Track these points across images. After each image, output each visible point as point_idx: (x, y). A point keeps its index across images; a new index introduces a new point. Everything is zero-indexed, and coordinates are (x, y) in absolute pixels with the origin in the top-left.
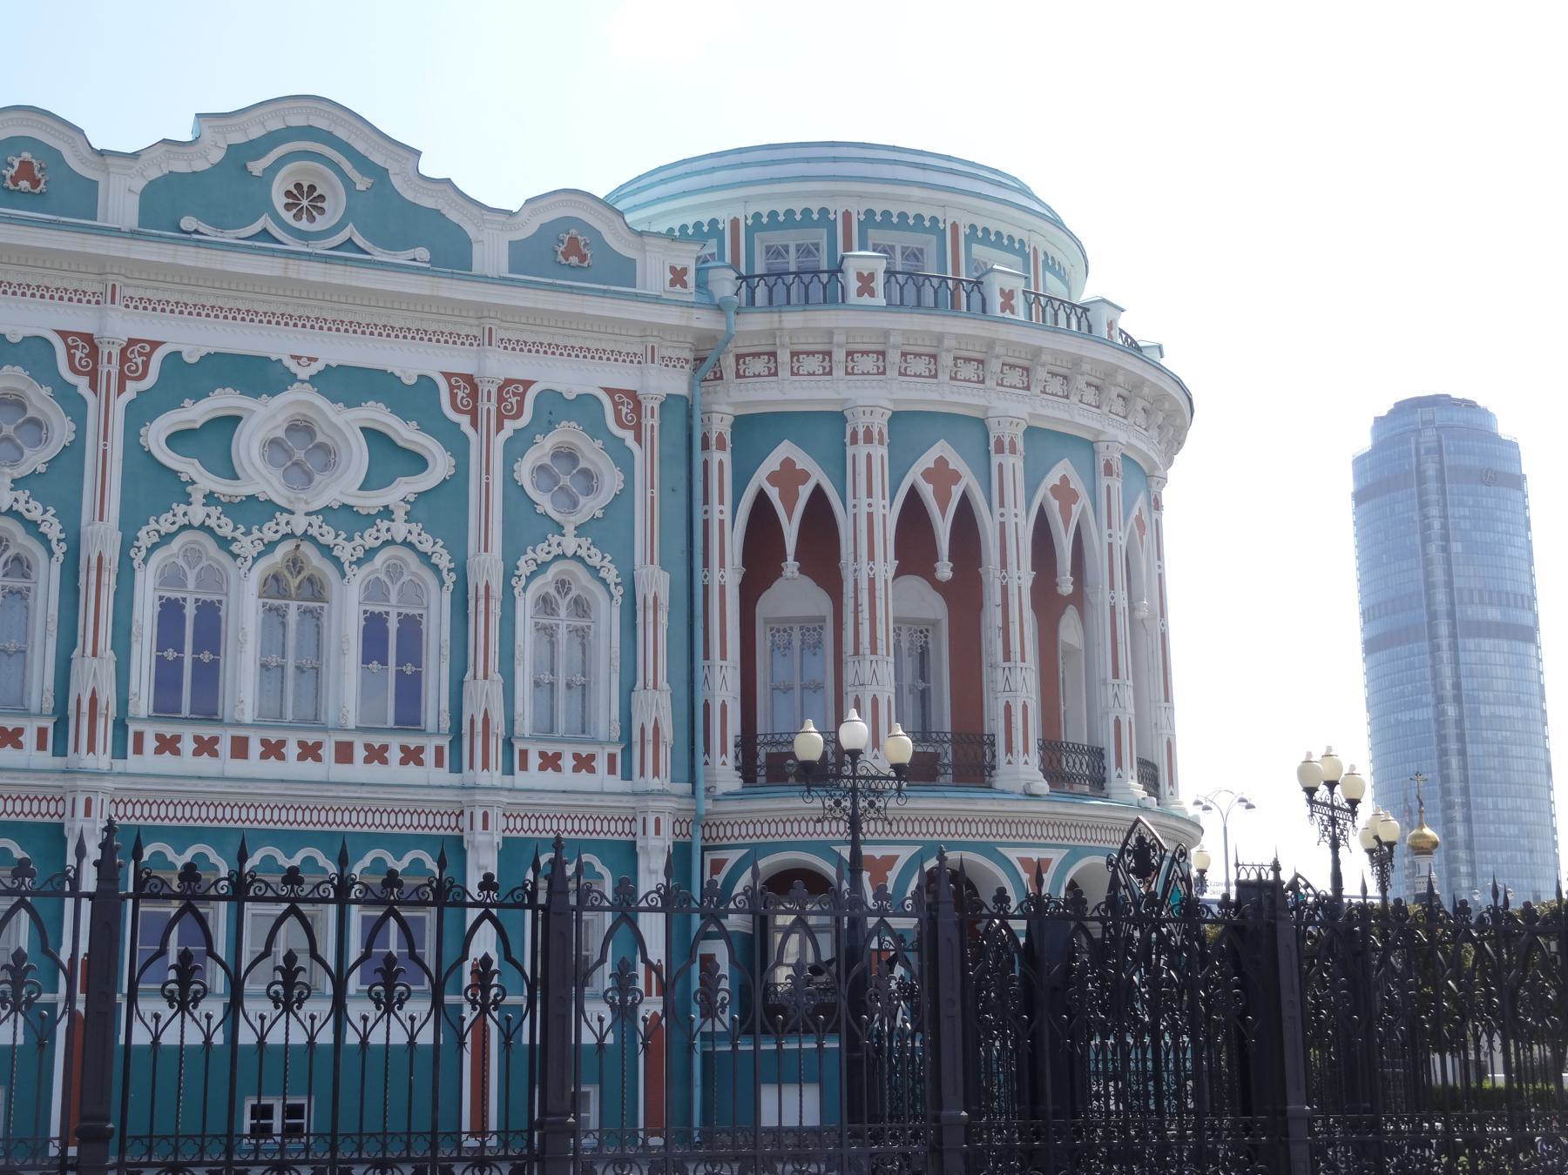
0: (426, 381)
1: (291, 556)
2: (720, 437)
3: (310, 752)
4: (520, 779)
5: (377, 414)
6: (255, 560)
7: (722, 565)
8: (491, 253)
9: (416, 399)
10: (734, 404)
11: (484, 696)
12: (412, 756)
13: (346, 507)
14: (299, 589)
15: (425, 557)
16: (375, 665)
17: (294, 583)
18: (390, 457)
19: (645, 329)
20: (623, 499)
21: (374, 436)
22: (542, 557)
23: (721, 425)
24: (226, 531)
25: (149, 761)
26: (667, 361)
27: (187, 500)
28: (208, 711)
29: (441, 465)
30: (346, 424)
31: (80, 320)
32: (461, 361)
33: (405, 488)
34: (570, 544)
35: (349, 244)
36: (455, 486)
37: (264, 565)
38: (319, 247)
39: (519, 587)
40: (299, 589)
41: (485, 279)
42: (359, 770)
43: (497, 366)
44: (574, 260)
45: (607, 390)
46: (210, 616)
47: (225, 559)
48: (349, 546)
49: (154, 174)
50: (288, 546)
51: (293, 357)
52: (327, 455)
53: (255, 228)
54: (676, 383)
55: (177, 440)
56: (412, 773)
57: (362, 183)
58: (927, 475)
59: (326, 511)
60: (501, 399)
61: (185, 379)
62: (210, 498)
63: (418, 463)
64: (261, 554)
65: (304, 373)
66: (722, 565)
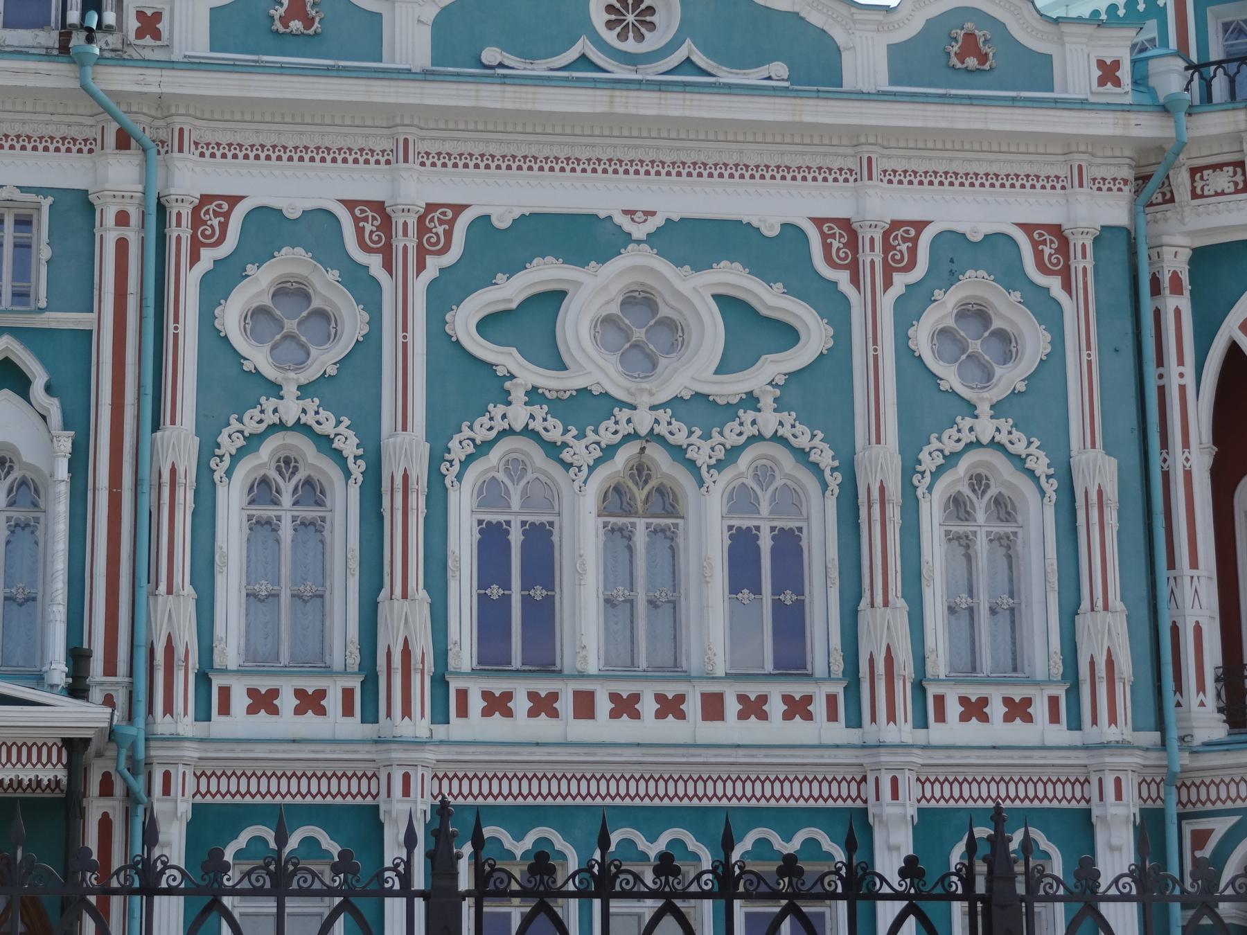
0: (791, 231)
1: (635, 462)
2: (1175, 277)
3: (670, 707)
4: (937, 733)
5: (732, 277)
6: (591, 469)
7: (1186, 444)
8: (866, 63)
9: (779, 253)
11: (885, 628)
12: (798, 708)
13: (700, 397)
14: (643, 502)
15: (802, 455)
16: (745, 594)
17: (640, 495)
18: (752, 331)
19: (1068, 143)
21: (727, 303)
22: (950, 446)
23: (1176, 262)
24: (555, 435)
25: (475, 725)
26: (1099, 184)
27: (505, 398)
29: (816, 336)
30: (694, 290)
31: (367, 184)
34: (986, 428)
35: (688, 64)
36: (835, 361)
37: (602, 473)
38: (650, 72)
39: (922, 484)
40: (643, 502)
41: (860, 96)
42: (732, 728)
43: (880, 205)
44: (972, 62)
45: (1022, 226)
46: (540, 540)
47: (555, 470)
48: (706, 446)
50: (631, 449)
51: (626, 212)
52: (673, 332)
53: (572, 54)
54: (1114, 210)
55: (489, 325)
56: (799, 731)
59: (675, 403)
60: (887, 247)
61: (497, 247)
62: (534, 395)
63: (788, 335)
64: (598, 462)
65: (639, 232)
66: (1186, 444)
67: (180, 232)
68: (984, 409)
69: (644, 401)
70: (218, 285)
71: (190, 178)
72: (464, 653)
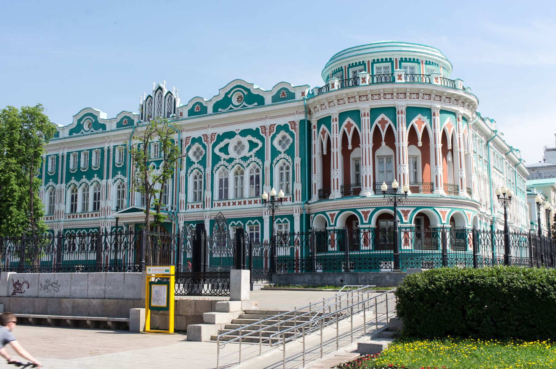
0: (257, 129)
5: (249, 137)
8: (268, 100)
9: (255, 133)
10: (316, 118)
13: (245, 156)
14: (239, 174)
18: (253, 145)
19: (294, 108)
20: (293, 144)
21: (250, 142)
24: (227, 165)
26: (300, 113)
27: (220, 160)
28: (226, 198)
30: (245, 141)
32: (262, 123)
33: (255, 150)
35: (244, 106)
37: (233, 169)
40: (239, 174)
46: (227, 180)
49: (214, 102)
54: (302, 117)
55: (221, 150)
57: (246, 93)
58: (346, 126)
60: (270, 129)
61: (220, 138)
62: (224, 160)
63: (257, 145)
65: (237, 133)
67: (184, 143)
68: (283, 153)
69: (237, 158)
70: (188, 150)
71: (184, 135)
72: (216, 197)
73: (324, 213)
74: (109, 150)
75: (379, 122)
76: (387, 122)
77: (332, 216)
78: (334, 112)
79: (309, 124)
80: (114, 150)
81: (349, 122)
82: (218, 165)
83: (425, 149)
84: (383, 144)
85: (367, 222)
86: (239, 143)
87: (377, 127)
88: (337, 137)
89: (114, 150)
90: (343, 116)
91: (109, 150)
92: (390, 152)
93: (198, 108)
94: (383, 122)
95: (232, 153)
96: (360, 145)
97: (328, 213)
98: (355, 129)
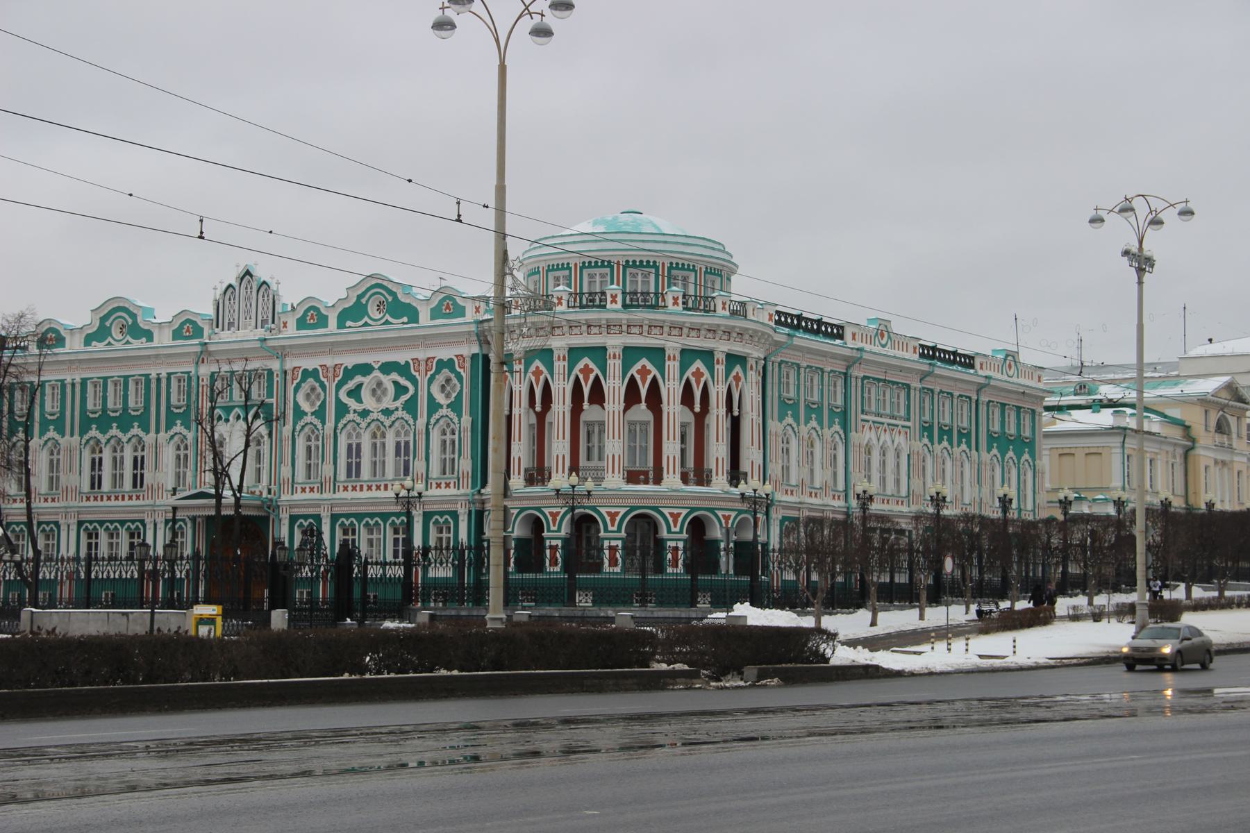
14: (378, 435)
40: (378, 435)
46: (359, 446)
55: (350, 394)
61: (349, 373)
62: (355, 411)
73: (538, 509)
74: (159, 380)
75: (638, 372)
76: (649, 372)
77: (554, 515)
78: (559, 344)
79: (486, 360)
80: (169, 379)
81: (586, 366)
82: (344, 421)
83: (701, 418)
84: (643, 405)
85: (615, 528)
86: (379, 384)
87: (632, 377)
88: (562, 389)
89: (169, 379)
90: (575, 353)
91: (159, 380)
92: (649, 416)
93: (312, 318)
94: (644, 372)
95: (369, 402)
96: (606, 405)
97: (546, 511)
98: (597, 378)
